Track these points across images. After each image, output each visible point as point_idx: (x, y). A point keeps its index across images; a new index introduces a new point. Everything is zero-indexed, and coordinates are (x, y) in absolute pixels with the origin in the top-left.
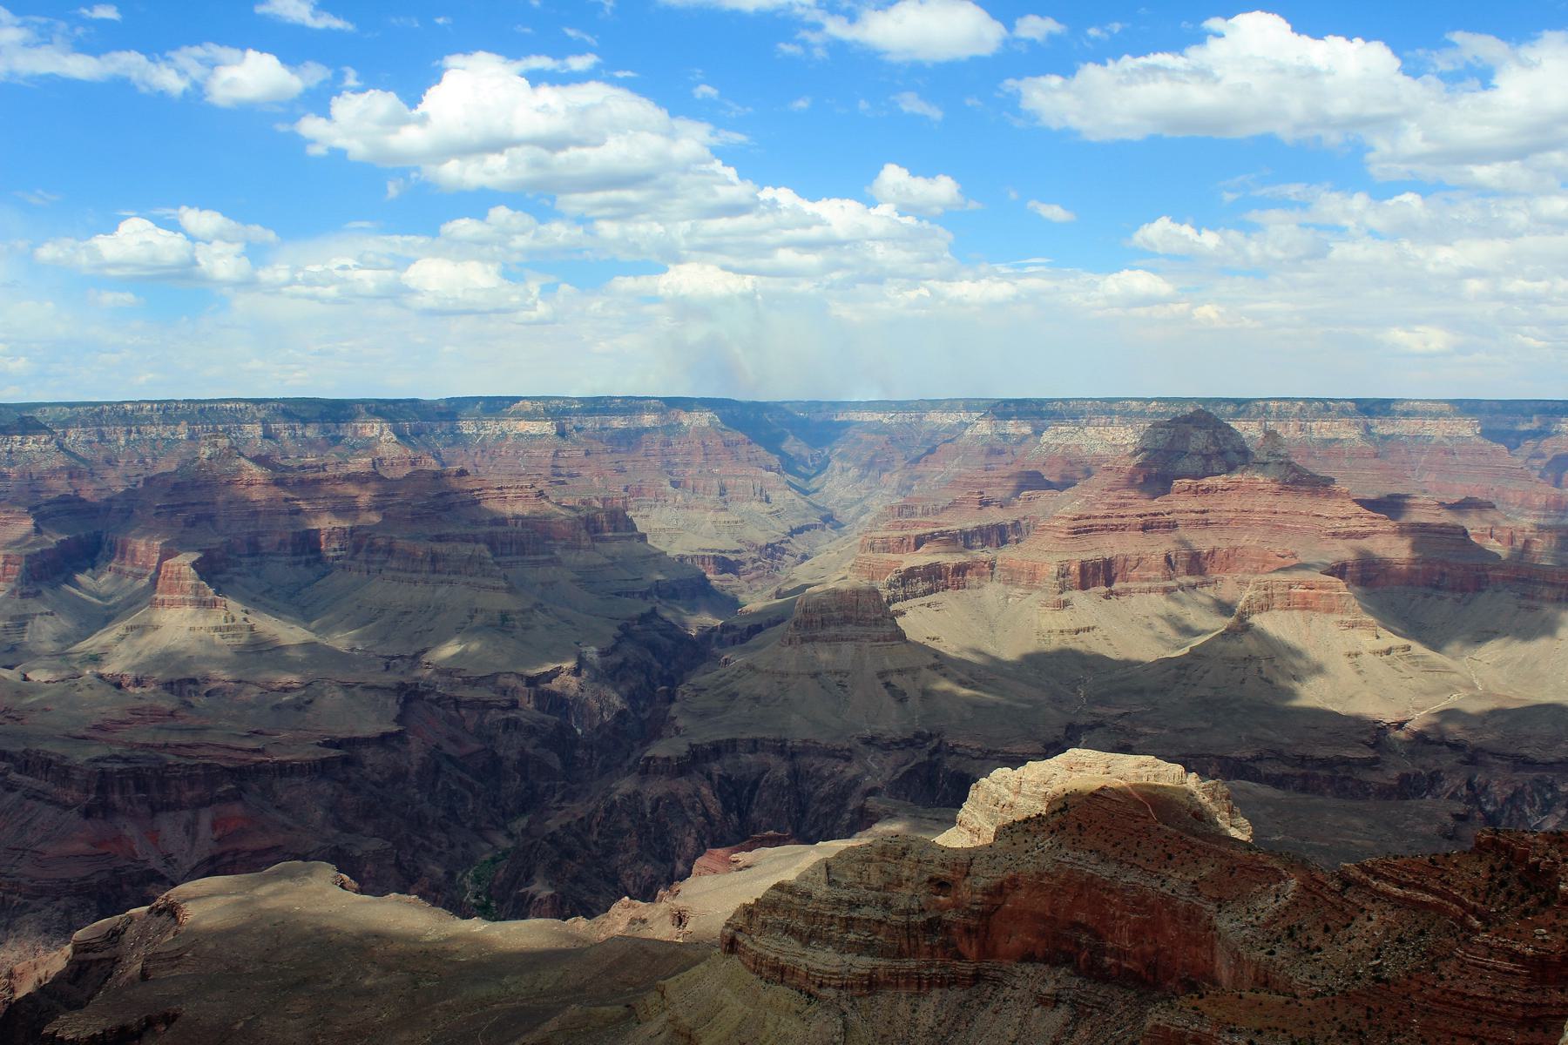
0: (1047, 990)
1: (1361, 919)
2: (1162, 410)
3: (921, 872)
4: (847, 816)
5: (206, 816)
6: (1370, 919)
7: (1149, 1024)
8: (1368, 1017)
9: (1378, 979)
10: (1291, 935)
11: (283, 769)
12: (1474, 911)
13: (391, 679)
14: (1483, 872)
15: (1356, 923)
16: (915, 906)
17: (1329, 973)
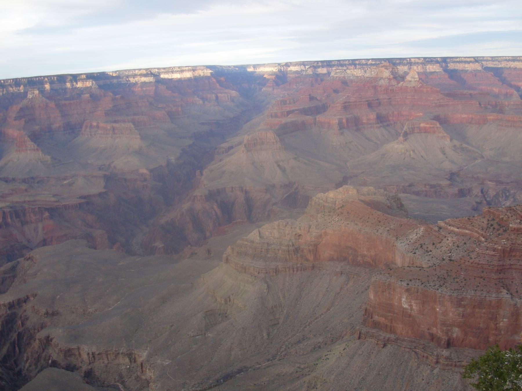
0: (338, 270)
1: (445, 240)
2: (373, 63)
4: (266, 213)
5: (40, 225)
6: (448, 240)
7: (373, 280)
8: (447, 273)
9: (451, 260)
10: (421, 247)
11: (66, 207)
12: (482, 235)
13: (102, 173)
14: (486, 222)
15: (443, 241)
16: (291, 244)
17: (434, 259)
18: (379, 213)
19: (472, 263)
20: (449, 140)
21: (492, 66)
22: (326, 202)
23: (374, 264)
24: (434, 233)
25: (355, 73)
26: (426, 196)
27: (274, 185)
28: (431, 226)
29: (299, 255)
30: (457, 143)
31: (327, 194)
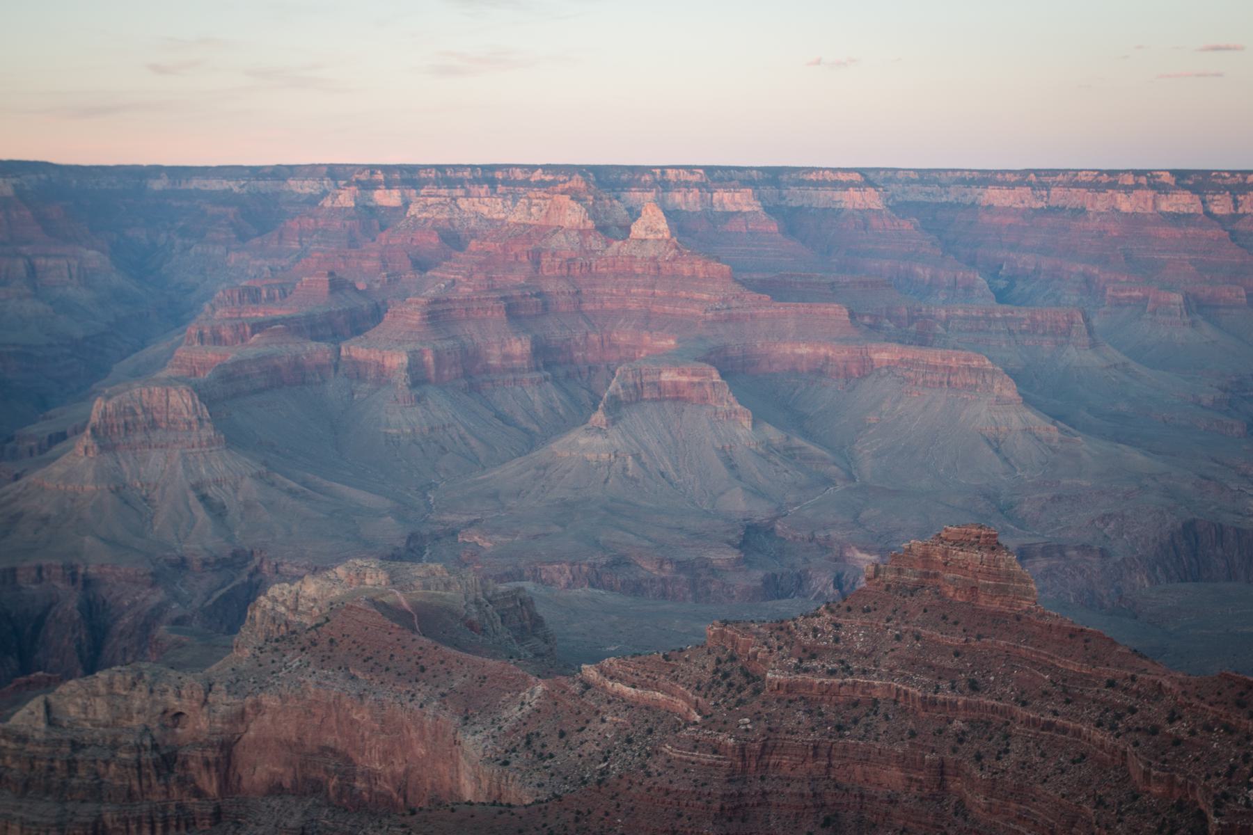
1: (595, 723)
2: (548, 178)
3: (155, 703)
6: (603, 721)
8: (577, 820)
10: (528, 743)
14: (710, 666)
15: (591, 726)
17: (557, 780)
18: (425, 641)
19: (649, 790)
20: (747, 423)
21: (921, 198)
22: (295, 610)
23: (401, 800)
24: (570, 703)
25: (485, 210)
26: (664, 595)
27: (183, 560)
28: (563, 680)
29: (172, 779)
30: (774, 434)
31: (299, 583)
